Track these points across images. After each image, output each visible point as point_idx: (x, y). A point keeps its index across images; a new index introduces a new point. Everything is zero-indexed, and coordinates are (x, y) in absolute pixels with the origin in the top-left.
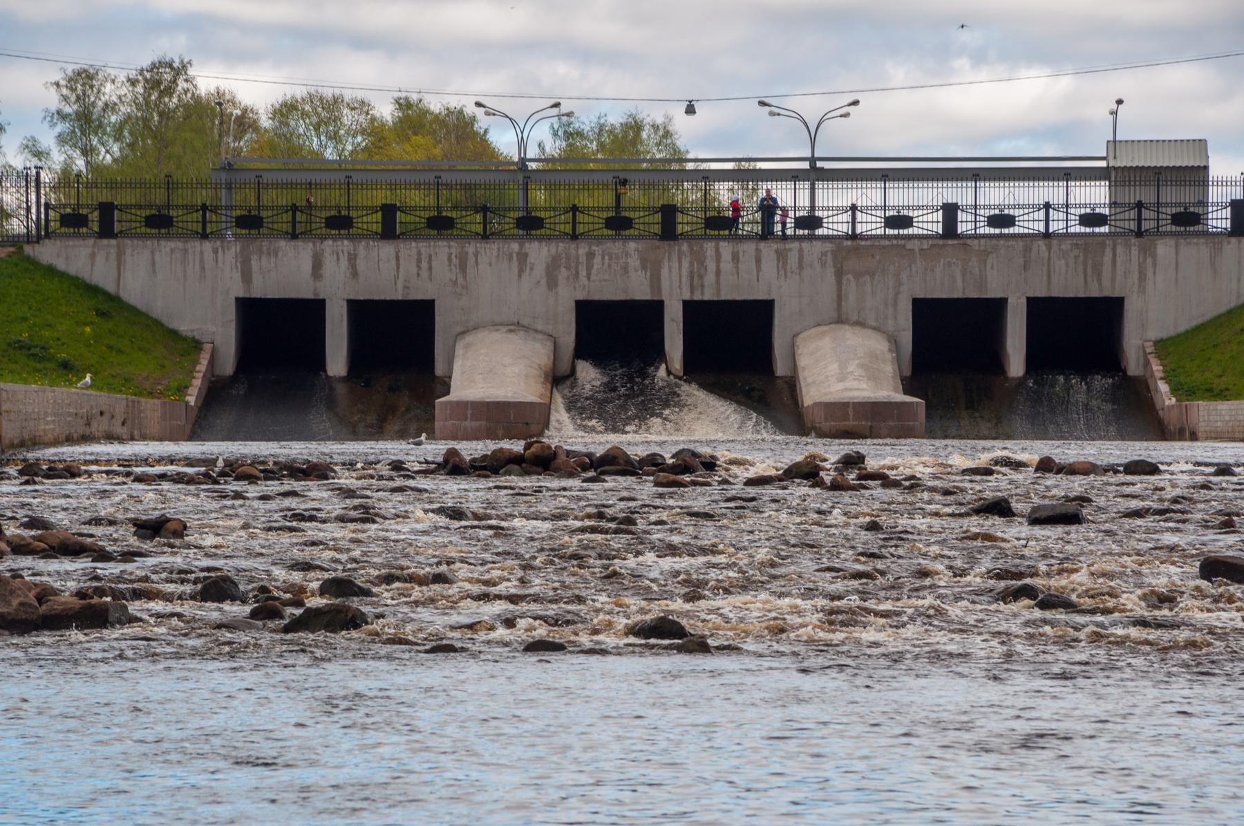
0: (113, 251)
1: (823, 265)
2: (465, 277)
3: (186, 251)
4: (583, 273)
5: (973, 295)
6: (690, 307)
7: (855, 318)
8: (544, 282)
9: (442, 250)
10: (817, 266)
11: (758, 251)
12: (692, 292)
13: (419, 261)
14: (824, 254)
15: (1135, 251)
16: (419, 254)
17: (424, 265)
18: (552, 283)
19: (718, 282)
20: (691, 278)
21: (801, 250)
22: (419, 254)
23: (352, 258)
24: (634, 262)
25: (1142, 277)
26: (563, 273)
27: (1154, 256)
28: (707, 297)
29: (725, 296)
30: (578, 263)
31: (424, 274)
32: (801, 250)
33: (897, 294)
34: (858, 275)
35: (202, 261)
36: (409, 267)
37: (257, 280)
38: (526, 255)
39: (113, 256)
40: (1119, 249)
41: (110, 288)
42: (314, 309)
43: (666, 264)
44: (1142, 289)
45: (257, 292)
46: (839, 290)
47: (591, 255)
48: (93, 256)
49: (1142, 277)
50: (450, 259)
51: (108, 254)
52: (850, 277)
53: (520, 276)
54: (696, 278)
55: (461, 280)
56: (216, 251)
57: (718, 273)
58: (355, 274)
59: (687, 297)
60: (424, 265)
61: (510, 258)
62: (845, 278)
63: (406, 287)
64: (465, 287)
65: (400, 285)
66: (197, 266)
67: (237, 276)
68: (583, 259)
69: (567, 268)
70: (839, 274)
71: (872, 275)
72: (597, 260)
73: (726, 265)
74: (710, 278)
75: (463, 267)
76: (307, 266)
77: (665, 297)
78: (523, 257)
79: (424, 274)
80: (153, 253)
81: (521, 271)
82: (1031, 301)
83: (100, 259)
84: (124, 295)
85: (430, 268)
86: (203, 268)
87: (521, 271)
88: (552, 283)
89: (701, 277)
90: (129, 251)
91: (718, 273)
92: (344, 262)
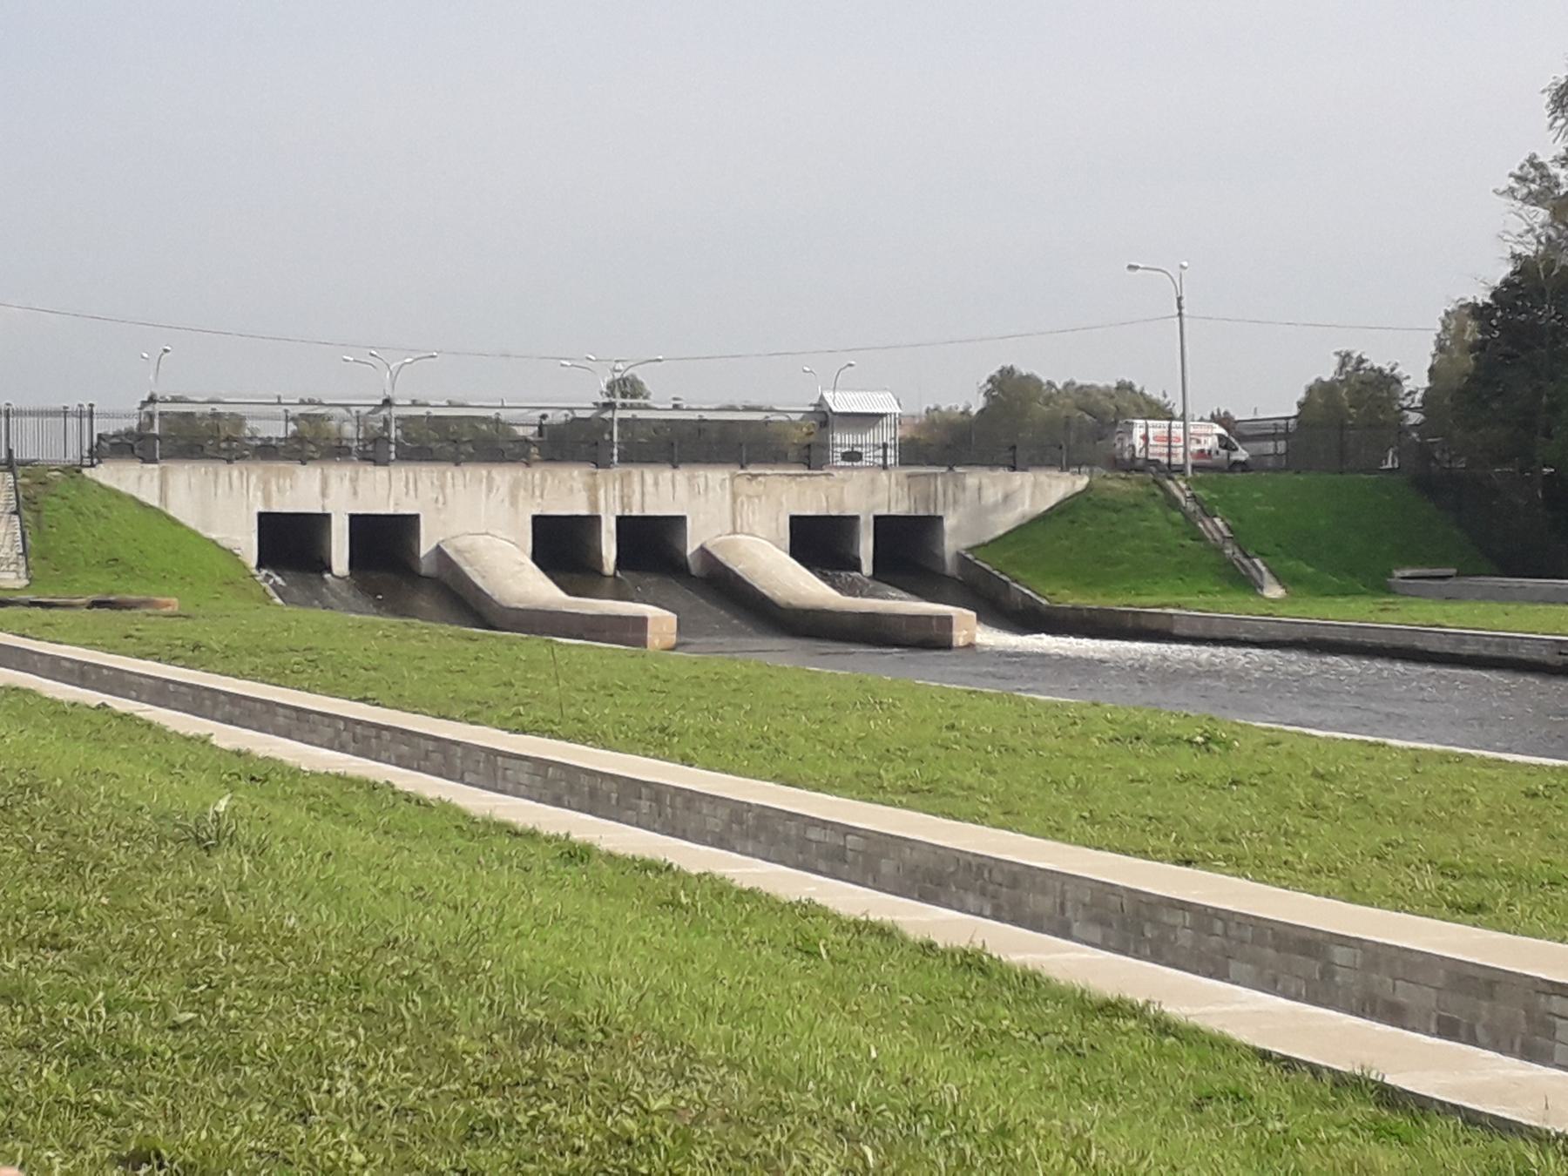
0: (157, 473)
2: (444, 497)
4: (537, 493)
5: (834, 513)
6: (621, 520)
8: (507, 504)
9: (426, 474)
11: (673, 476)
12: (623, 510)
23: (354, 481)
26: (522, 493)
28: (635, 513)
29: (649, 512)
31: (412, 492)
32: (706, 477)
34: (749, 497)
41: (156, 504)
45: (276, 509)
47: (544, 479)
53: (488, 496)
54: (625, 500)
55: (441, 499)
57: (643, 494)
58: (355, 493)
59: (619, 513)
61: (481, 481)
62: (739, 501)
63: (396, 504)
65: (392, 503)
69: (525, 490)
70: (734, 496)
71: (759, 497)
74: (637, 497)
77: (602, 513)
78: (490, 479)
79: (412, 492)
81: (490, 490)
82: (876, 518)
84: (171, 512)
85: (416, 490)
87: (490, 490)
88: (514, 501)
89: (629, 498)
91: (643, 494)
92: (347, 482)
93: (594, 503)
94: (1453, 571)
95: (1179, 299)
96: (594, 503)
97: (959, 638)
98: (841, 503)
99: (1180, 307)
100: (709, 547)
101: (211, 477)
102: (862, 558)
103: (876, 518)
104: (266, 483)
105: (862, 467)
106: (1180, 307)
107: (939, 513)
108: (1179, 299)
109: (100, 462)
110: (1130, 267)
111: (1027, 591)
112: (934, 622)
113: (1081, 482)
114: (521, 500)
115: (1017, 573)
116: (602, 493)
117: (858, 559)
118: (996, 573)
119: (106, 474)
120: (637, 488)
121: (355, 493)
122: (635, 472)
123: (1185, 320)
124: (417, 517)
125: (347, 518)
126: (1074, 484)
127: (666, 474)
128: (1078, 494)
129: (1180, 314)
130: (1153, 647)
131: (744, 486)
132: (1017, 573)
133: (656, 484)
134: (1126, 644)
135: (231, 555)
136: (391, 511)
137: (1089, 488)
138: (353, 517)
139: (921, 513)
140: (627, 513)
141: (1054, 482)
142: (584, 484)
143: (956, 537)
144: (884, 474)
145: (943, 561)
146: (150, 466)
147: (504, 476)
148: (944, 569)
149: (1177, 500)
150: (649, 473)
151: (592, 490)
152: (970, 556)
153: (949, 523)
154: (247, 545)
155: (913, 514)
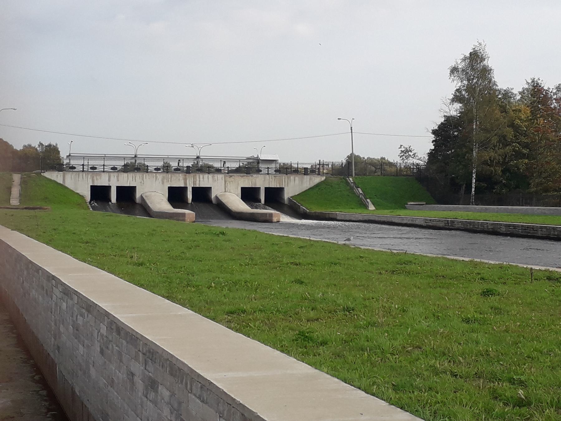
0: (62, 175)
1: (222, 179)
5: (253, 186)
6: (194, 189)
8: (161, 182)
9: (138, 175)
10: (221, 180)
14: (222, 177)
17: (134, 179)
20: (194, 182)
23: (118, 177)
26: (165, 180)
28: (197, 186)
34: (230, 182)
41: (62, 183)
42: (108, 188)
43: (188, 179)
47: (171, 177)
51: (61, 175)
52: (228, 182)
53: (156, 181)
54: (194, 183)
55: (142, 182)
57: (199, 181)
58: (118, 180)
59: (193, 186)
60: (134, 179)
61: (154, 177)
63: (130, 183)
64: (143, 183)
66: (82, 179)
68: (170, 177)
70: (225, 182)
71: (232, 182)
72: (173, 177)
73: (201, 179)
74: (198, 182)
76: (107, 179)
77: (188, 186)
82: (265, 188)
84: (66, 185)
88: (163, 183)
89: (196, 182)
91: (199, 181)
93: (185, 183)
94: (425, 203)
95: (351, 128)
96: (185, 183)
97: (275, 219)
98: (255, 184)
99: (351, 130)
100: (218, 196)
103: (265, 188)
105: (261, 174)
106: (351, 130)
107: (283, 187)
108: (351, 128)
109: (46, 171)
110: (339, 119)
111: (304, 208)
112: (268, 215)
113: (323, 178)
114: (165, 182)
115: (302, 202)
116: (188, 181)
117: (260, 200)
118: (297, 203)
121: (118, 180)
123: (353, 133)
124: (135, 187)
125: (116, 187)
126: (321, 179)
128: (322, 181)
129: (352, 132)
130: (332, 222)
131: (228, 179)
132: (302, 202)
133: (203, 178)
134: (327, 222)
135: (82, 197)
137: (325, 180)
138: (117, 187)
139: (278, 186)
140: (195, 186)
143: (287, 195)
144: (268, 176)
145: (284, 199)
146: (60, 172)
148: (285, 202)
149: (349, 183)
151: (185, 180)
152: (291, 199)
154: (87, 194)
155: (276, 187)
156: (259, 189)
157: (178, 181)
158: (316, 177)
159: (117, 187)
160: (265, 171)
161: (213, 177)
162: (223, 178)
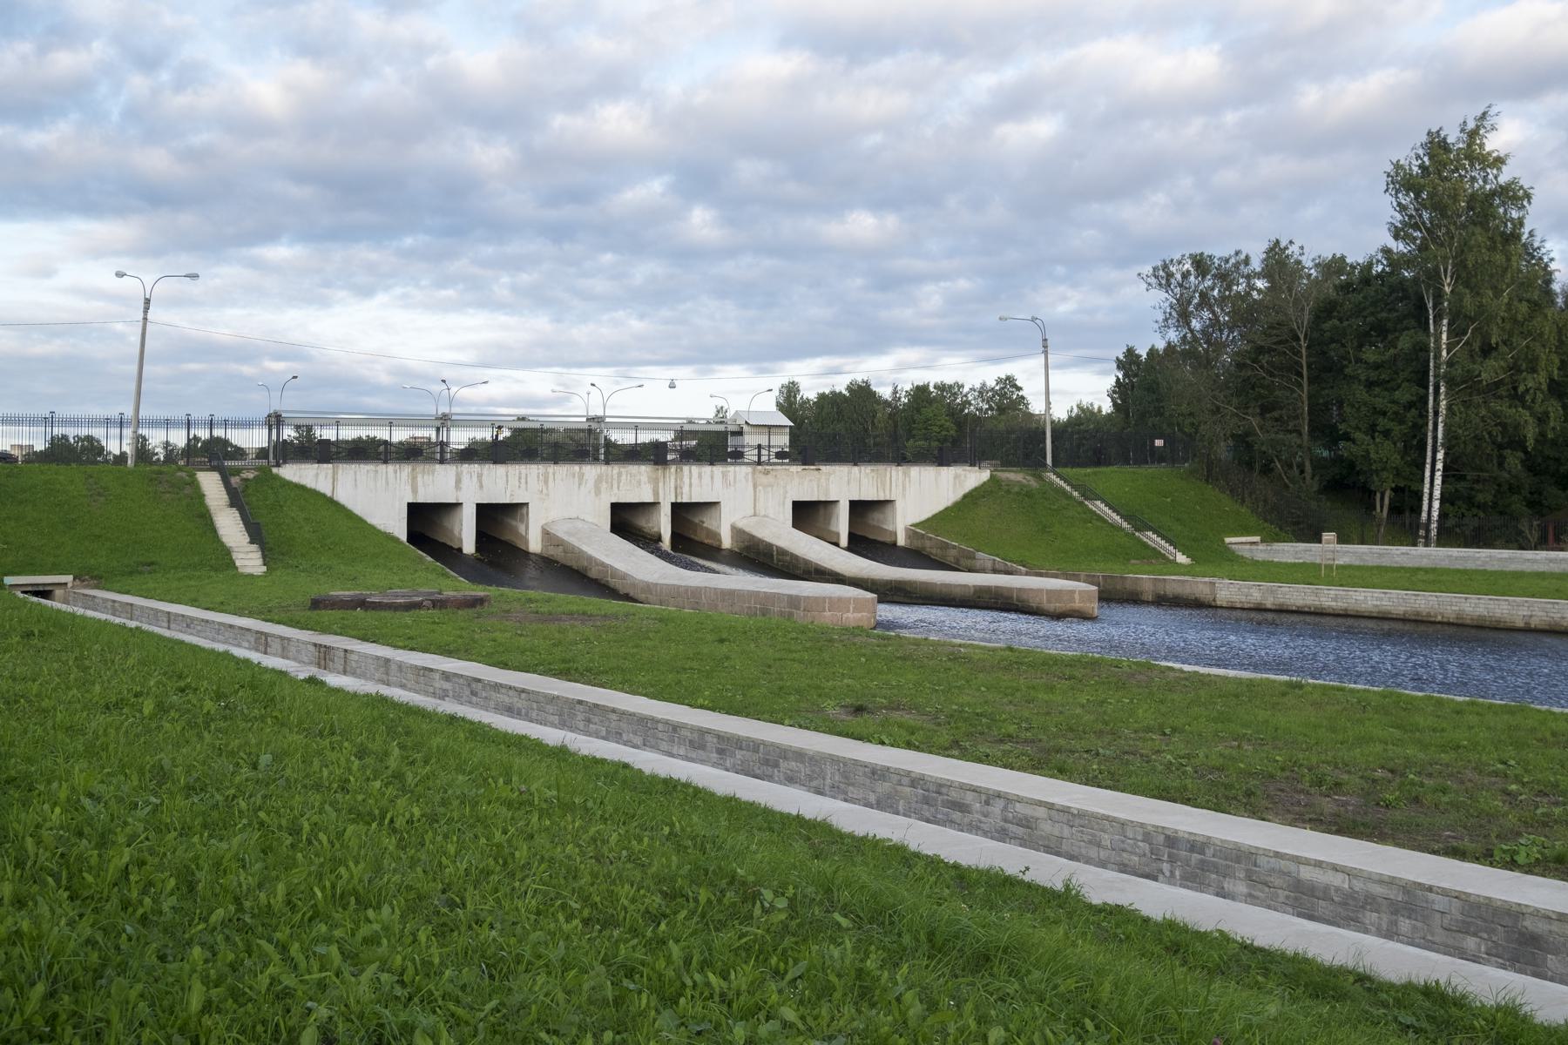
0: (330, 472)
1: (747, 481)
3: (376, 471)
4: (615, 486)
7: (763, 513)
8: (593, 494)
9: (533, 471)
12: (676, 498)
13: (520, 478)
14: (747, 474)
15: (901, 474)
16: (520, 473)
17: (523, 481)
18: (598, 492)
19: (690, 491)
20: (676, 488)
21: (735, 472)
22: (520, 473)
23: (480, 476)
24: (644, 478)
25: (904, 487)
26: (604, 485)
27: (910, 477)
28: (684, 501)
30: (612, 479)
31: (523, 485)
32: (735, 472)
33: (785, 498)
35: (387, 478)
36: (514, 481)
37: (421, 490)
38: (583, 474)
39: (330, 476)
40: (894, 473)
41: (329, 494)
44: (904, 496)
45: (421, 499)
46: (755, 496)
47: (620, 475)
48: (317, 475)
49: (904, 487)
50: (538, 477)
51: (327, 473)
53: (580, 484)
55: (545, 491)
56: (396, 472)
57: (691, 485)
58: (481, 486)
59: (673, 501)
60: (523, 481)
61: (574, 477)
63: (512, 495)
64: (547, 495)
65: (508, 495)
67: (409, 488)
68: (615, 477)
69: (607, 482)
70: (755, 487)
71: (772, 486)
72: (624, 477)
73: (695, 480)
74: (686, 489)
75: (546, 482)
76: (452, 482)
78: (581, 476)
79: (523, 485)
80: (355, 473)
83: (321, 477)
86: (387, 483)
88: (598, 492)
90: (340, 472)
91: (691, 485)
92: (475, 479)
93: (656, 493)
96: (656, 493)
100: (740, 525)
101: (372, 474)
102: (841, 533)
104: (414, 479)
109: (285, 462)
114: (603, 490)
116: (661, 485)
119: (291, 472)
120: (686, 480)
121: (481, 486)
122: (686, 468)
127: (707, 469)
131: (763, 479)
133: (700, 476)
135: (396, 540)
136: (508, 502)
138: (478, 505)
140: (679, 501)
141: (968, 475)
142: (649, 477)
146: (325, 465)
147: (591, 471)
150: (695, 469)
151: (655, 482)
153: (899, 505)
154: (400, 530)
156: (833, 503)
157: (635, 484)
158: (970, 471)
159: (478, 505)
160: (751, 455)
161: (724, 475)
162: (750, 476)
